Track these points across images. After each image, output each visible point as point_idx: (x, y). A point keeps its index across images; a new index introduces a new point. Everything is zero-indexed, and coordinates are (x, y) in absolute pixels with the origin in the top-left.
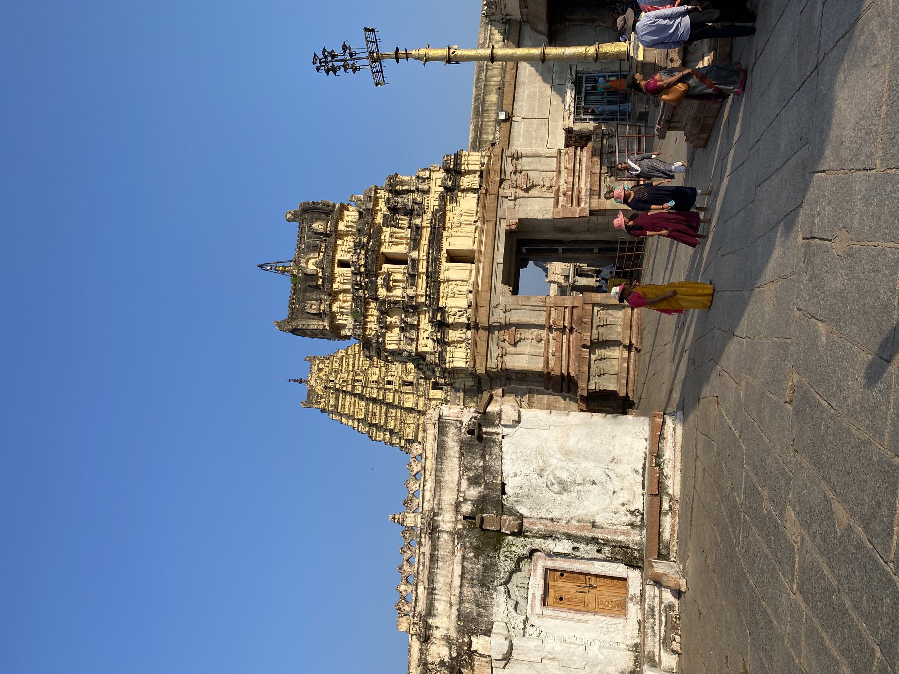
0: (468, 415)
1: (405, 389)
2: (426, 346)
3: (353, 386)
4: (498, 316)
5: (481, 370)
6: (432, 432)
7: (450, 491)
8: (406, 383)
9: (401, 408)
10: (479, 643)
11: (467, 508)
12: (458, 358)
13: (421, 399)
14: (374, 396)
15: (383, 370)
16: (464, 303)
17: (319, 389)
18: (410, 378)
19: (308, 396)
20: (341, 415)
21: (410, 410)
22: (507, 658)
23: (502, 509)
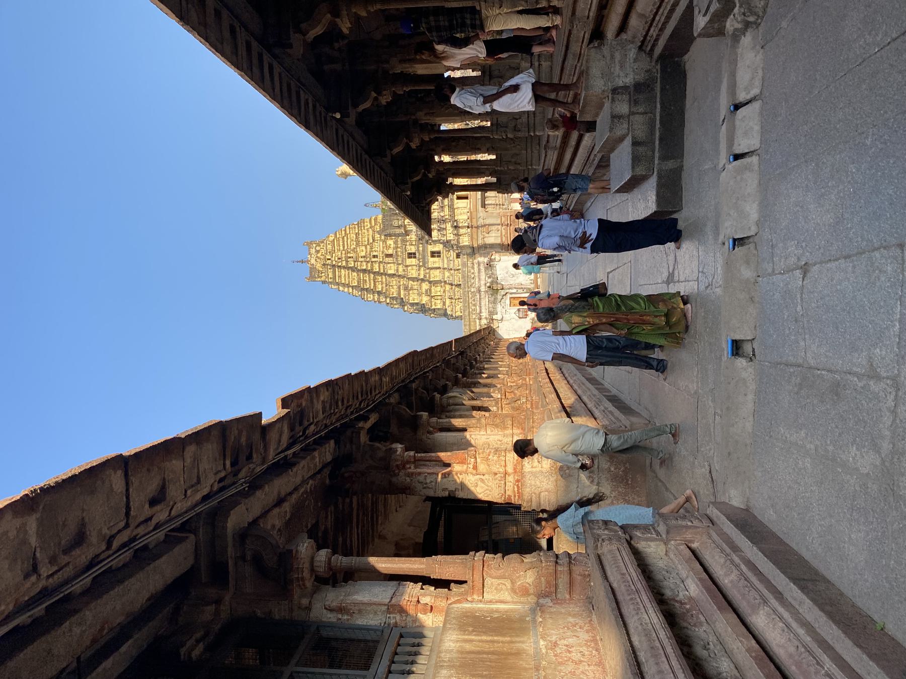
0: (486, 260)
1: (387, 260)
2: (450, 237)
3: (347, 261)
4: (481, 222)
5: (475, 245)
6: (476, 266)
7: (483, 281)
9: (386, 274)
10: (495, 317)
11: (488, 285)
12: (465, 241)
13: (400, 266)
14: (364, 267)
15: (368, 247)
16: (465, 217)
17: (319, 266)
18: (390, 252)
19: (311, 272)
20: (338, 284)
21: (393, 275)
22: (502, 320)
23: (497, 283)
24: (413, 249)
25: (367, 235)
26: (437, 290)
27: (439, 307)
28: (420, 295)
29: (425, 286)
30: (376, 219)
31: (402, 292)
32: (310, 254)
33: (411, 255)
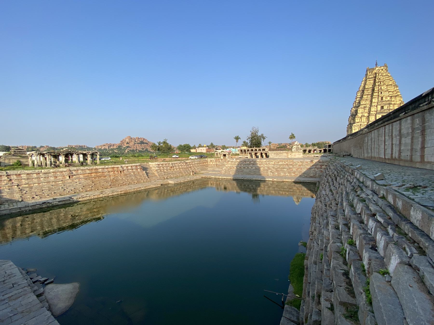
1: (380, 98)
3: (379, 82)
8: (382, 98)
13: (376, 104)
14: (375, 89)
17: (375, 71)
18: (384, 99)
20: (366, 80)
21: (371, 101)
24: (385, 108)
25: (392, 89)
26: (364, 119)
27: (356, 121)
28: (362, 113)
29: (366, 115)
30: (398, 92)
31: (363, 106)
32: (380, 67)
33: (382, 107)
